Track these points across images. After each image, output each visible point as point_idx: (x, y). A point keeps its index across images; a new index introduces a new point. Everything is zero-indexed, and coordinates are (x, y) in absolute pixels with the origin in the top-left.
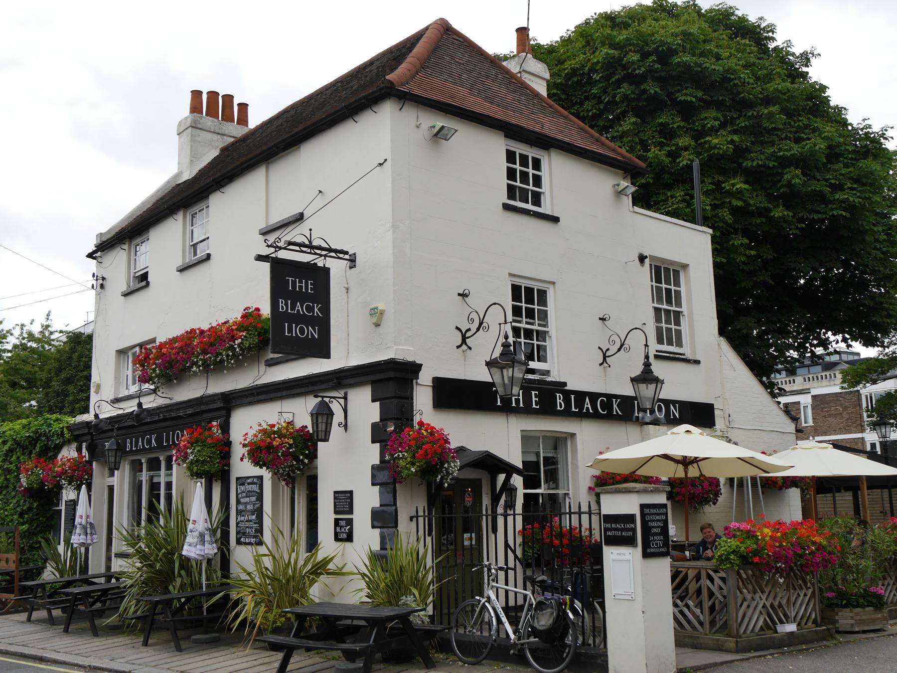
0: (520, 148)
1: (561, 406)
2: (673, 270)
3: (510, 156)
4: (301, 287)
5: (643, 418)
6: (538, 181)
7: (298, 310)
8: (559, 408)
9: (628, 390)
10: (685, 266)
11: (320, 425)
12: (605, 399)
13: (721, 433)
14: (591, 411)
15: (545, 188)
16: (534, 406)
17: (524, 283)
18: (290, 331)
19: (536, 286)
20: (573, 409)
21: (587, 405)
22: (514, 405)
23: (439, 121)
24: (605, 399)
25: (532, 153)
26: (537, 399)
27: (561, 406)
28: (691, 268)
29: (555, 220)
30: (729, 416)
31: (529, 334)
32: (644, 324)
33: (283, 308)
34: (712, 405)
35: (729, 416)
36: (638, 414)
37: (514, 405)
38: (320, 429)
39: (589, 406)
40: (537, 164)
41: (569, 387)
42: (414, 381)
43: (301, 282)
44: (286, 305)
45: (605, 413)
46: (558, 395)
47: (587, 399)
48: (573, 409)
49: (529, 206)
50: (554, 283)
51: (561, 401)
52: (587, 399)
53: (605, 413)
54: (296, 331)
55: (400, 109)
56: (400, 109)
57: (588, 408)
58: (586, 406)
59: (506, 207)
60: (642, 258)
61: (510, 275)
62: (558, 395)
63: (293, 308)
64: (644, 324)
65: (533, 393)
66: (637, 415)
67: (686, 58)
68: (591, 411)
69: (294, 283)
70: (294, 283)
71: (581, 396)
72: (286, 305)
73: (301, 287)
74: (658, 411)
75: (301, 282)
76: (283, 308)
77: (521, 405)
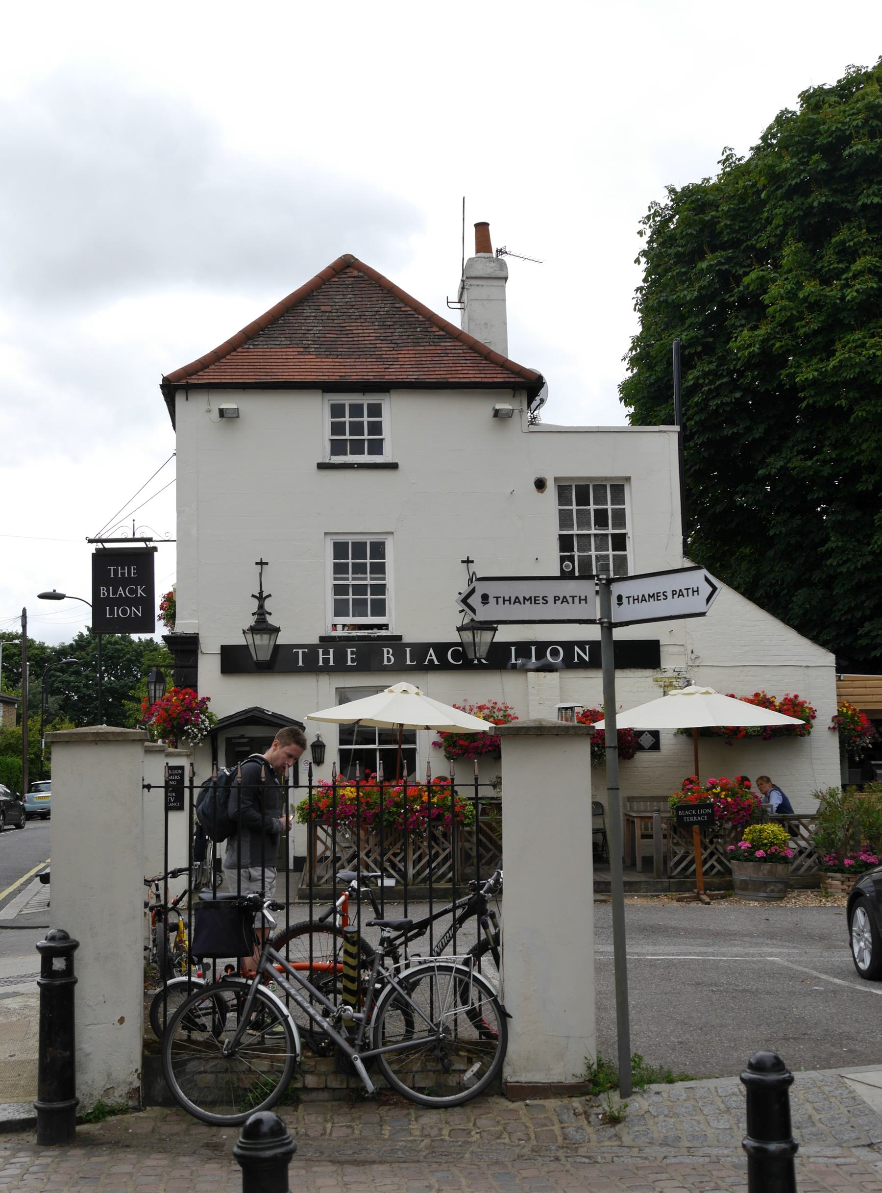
0: (347, 400)
1: (389, 660)
2: (611, 486)
3: (337, 411)
4: (123, 574)
5: (523, 665)
6: (376, 428)
7: (121, 594)
8: (386, 663)
9: (455, 638)
10: (628, 479)
11: (157, 692)
12: (461, 649)
13: (676, 674)
14: (436, 662)
15: (387, 433)
16: (349, 663)
17: (350, 539)
18: (112, 612)
19: (368, 539)
20: (408, 662)
21: (431, 656)
22: (321, 663)
23: (229, 403)
24: (461, 649)
25: (365, 400)
26: (354, 656)
27: (389, 660)
28: (632, 480)
29: (394, 466)
30: (692, 652)
31: (360, 589)
32: (537, 559)
33: (104, 594)
34: (659, 641)
35: (692, 652)
36: (516, 660)
37: (321, 663)
38: (157, 695)
39: (434, 657)
40: (376, 410)
41: (405, 640)
42: (199, 651)
43: (123, 569)
44: (108, 591)
45: (461, 663)
46: (385, 650)
47: (431, 651)
48: (408, 662)
49: (366, 458)
50: (392, 533)
51: (389, 655)
52: (431, 651)
53: (461, 663)
54: (118, 612)
55: (187, 399)
56: (187, 399)
57: (431, 661)
58: (428, 658)
59: (322, 466)
60: (540, 484)
61: (326, 534)
62: (385, 650)
63: (115, 593)
64: (537, 559)
65: (349, 650)
66: (513, 661)
67: (858, 147)
68: (436, 662)
69: (116, 571)
70: (116, 571)
71: (420, 649)
72: (108, 591)
73: (123, 574)
74: (551, 655)
75: (123, 569)
76: (104, 594)
77: (331, 663)
